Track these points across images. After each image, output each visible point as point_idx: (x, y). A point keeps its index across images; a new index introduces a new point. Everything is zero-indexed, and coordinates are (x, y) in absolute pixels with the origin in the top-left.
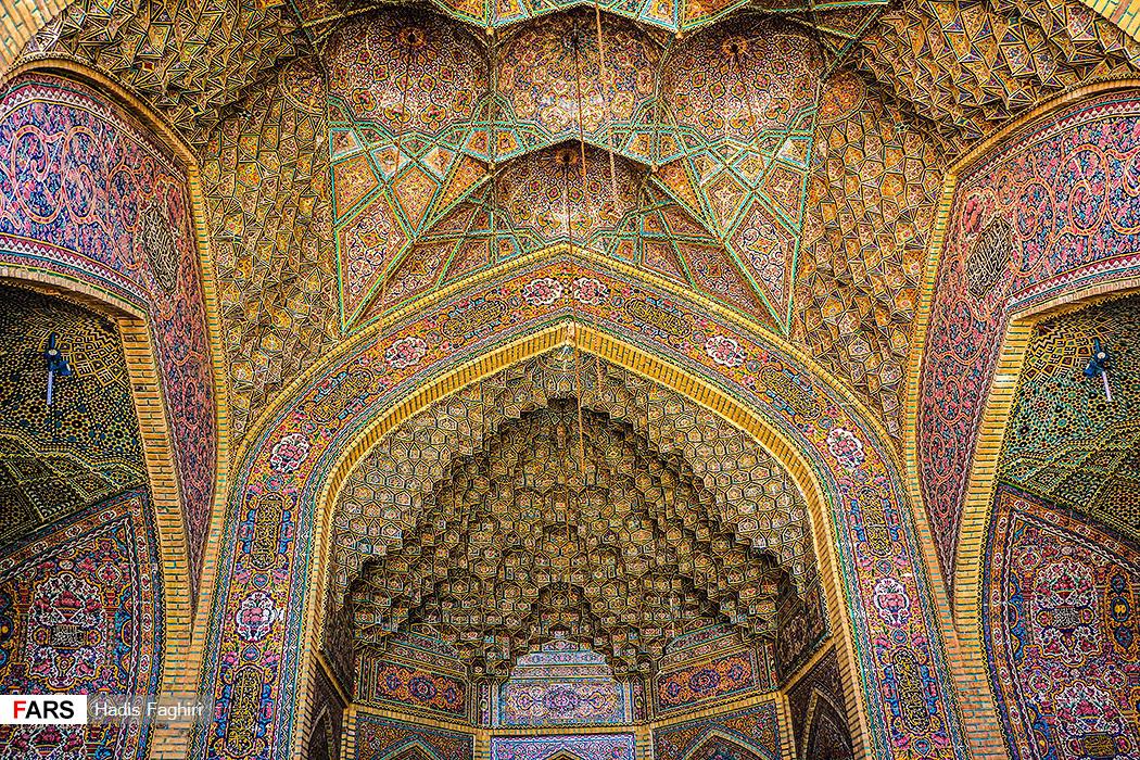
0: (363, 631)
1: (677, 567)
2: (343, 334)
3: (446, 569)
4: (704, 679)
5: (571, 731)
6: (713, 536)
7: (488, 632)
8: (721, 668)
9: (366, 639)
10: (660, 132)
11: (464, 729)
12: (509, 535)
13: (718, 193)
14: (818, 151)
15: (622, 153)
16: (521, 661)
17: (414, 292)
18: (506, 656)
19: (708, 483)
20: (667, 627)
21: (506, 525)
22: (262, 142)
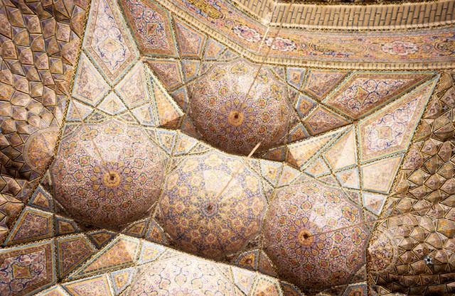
2: (439, 75)
10: (170, 153)
13: (139, 93)
14: (62, 110)
15: (198, 142)
17: (372, 77)
22: (425, 236)
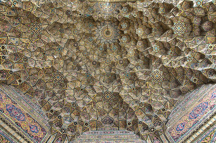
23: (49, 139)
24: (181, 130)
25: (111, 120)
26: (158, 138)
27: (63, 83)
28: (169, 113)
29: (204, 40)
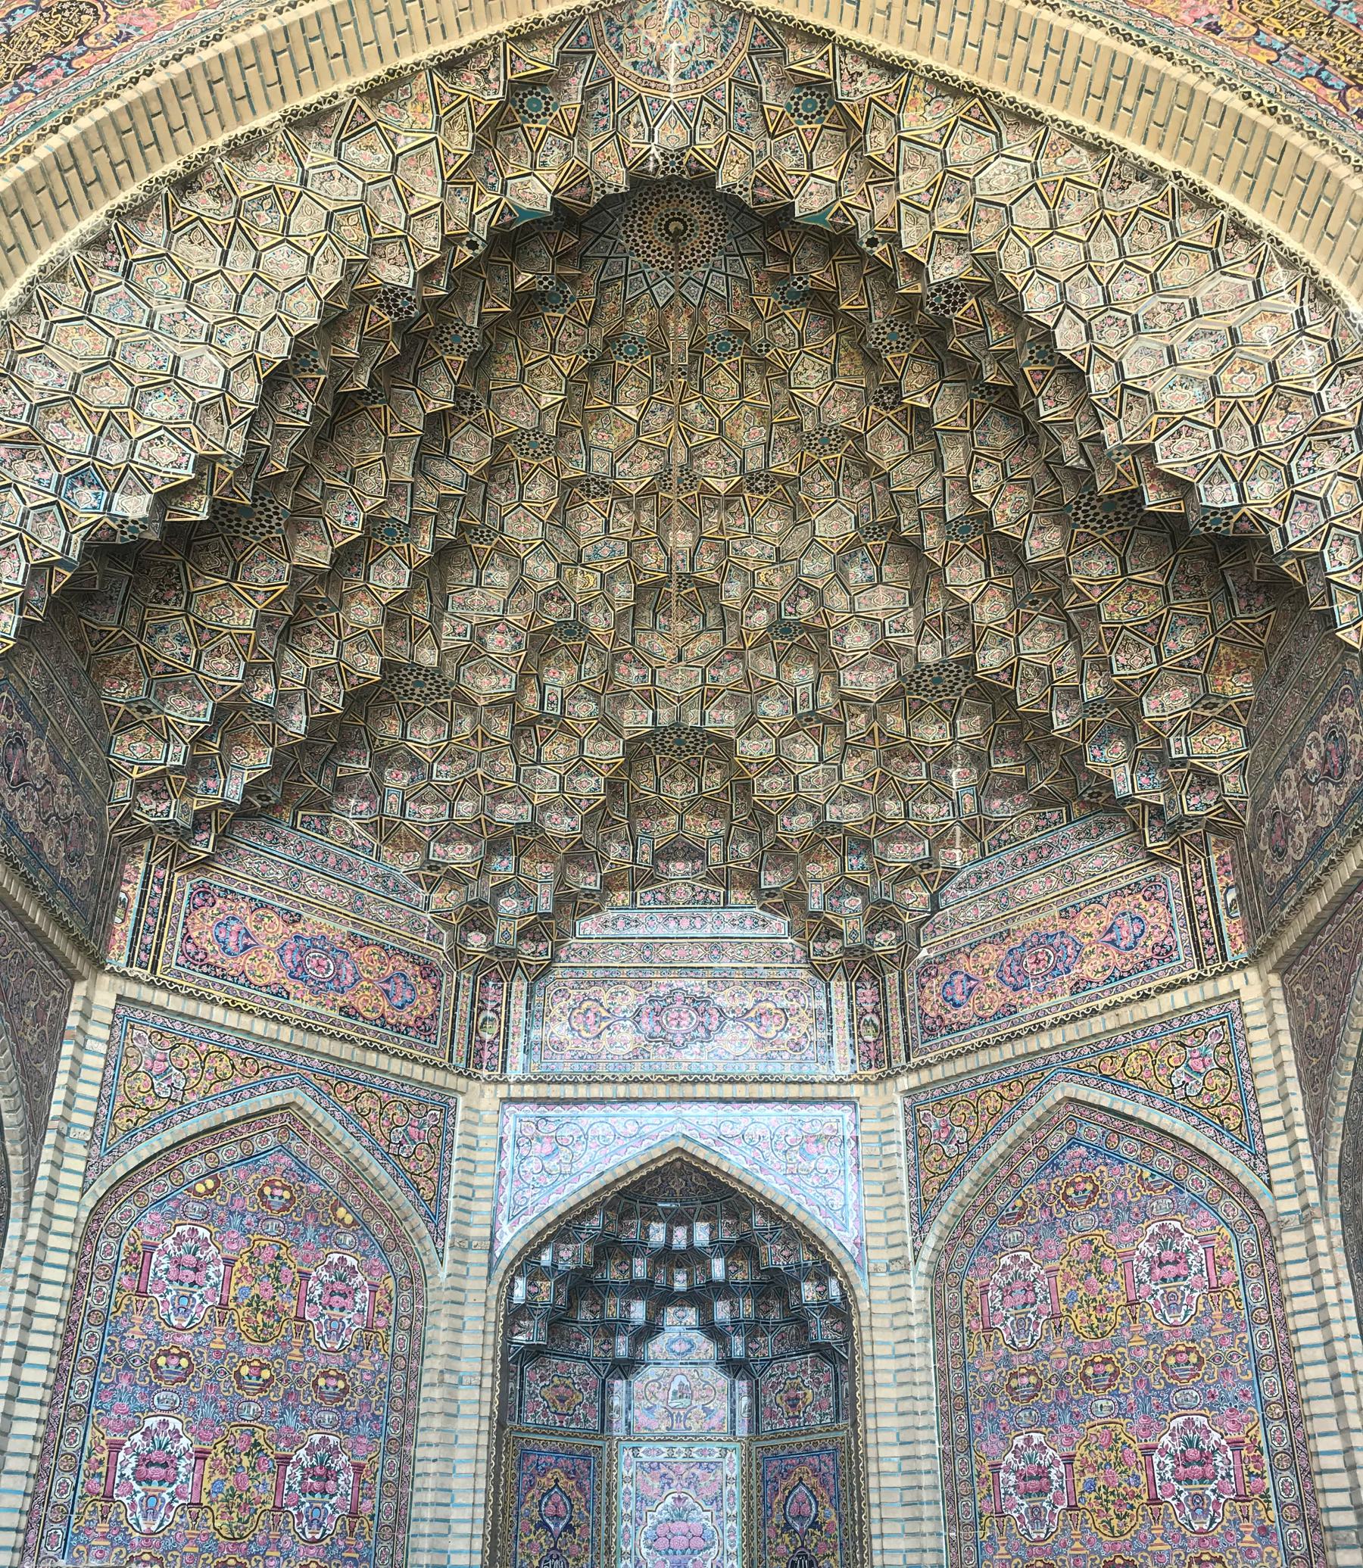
0: (139, 786)
1: (972, 660)
3: (376, 658)
4: (1043, 955)
5: (701, 1091)
6: (1071, 544)
7: (498, 842)
8: (1087, 925)
9: (151, 810)
11: (430, 1075)
12: (548, 596)
16: (588, 926)
18: (546, 905)
19: (1068, 339)
20: (942, 839)
21: (542, 570)
23: (456, 998)
24: (955, 1005)
25: (694, 850)
26: (875, 978)
27: (449, 701)
28: (951, 873)
29: (1198, 654)
